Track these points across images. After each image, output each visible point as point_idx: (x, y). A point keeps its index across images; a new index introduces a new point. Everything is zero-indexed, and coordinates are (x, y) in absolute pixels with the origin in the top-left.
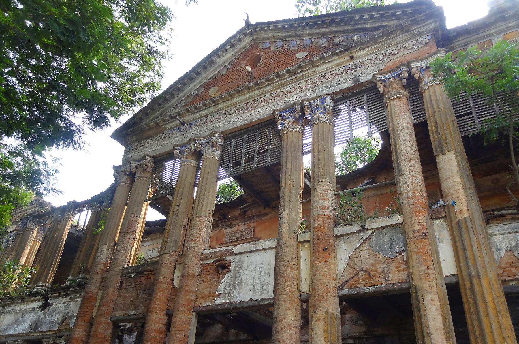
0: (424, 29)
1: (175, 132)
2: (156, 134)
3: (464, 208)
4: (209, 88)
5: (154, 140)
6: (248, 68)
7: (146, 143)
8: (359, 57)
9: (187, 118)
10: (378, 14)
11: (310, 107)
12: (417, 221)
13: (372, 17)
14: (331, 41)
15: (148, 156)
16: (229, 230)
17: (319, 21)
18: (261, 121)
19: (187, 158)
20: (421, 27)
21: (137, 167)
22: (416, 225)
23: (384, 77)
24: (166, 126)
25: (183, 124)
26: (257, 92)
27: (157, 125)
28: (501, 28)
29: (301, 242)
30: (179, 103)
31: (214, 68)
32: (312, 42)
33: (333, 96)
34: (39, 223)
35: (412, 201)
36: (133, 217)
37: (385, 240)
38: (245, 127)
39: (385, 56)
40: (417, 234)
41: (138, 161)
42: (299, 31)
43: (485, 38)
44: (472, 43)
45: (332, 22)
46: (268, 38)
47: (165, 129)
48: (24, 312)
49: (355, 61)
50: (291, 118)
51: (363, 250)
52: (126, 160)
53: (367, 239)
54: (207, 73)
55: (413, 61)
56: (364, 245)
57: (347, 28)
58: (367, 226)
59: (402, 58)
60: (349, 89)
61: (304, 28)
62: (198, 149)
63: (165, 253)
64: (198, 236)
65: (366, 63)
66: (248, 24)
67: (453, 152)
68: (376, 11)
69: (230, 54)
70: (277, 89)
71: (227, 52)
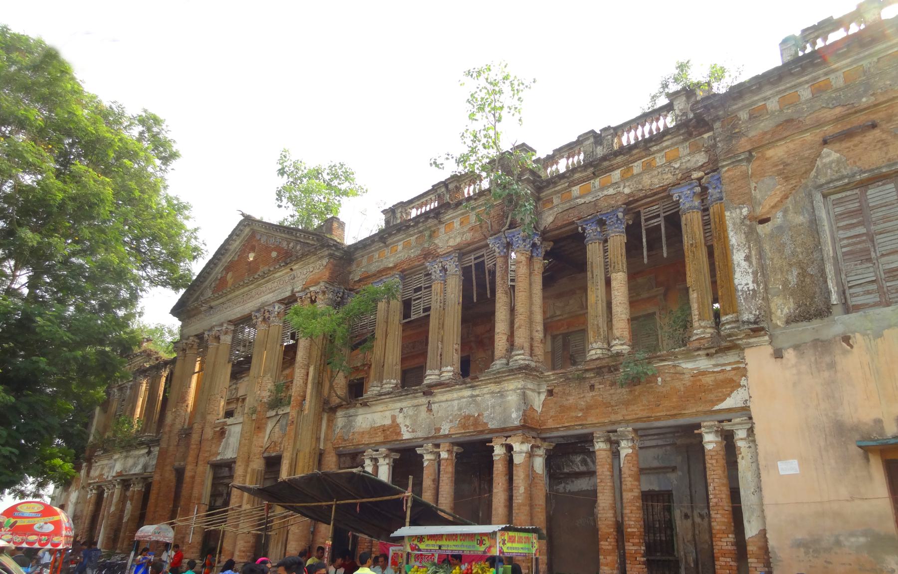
9: (213, 304)
25: (211, 308)
26: (246, 289)
33: (281, 302)
34: (145, 377)
48: (139, 457)
69: (238, 242)
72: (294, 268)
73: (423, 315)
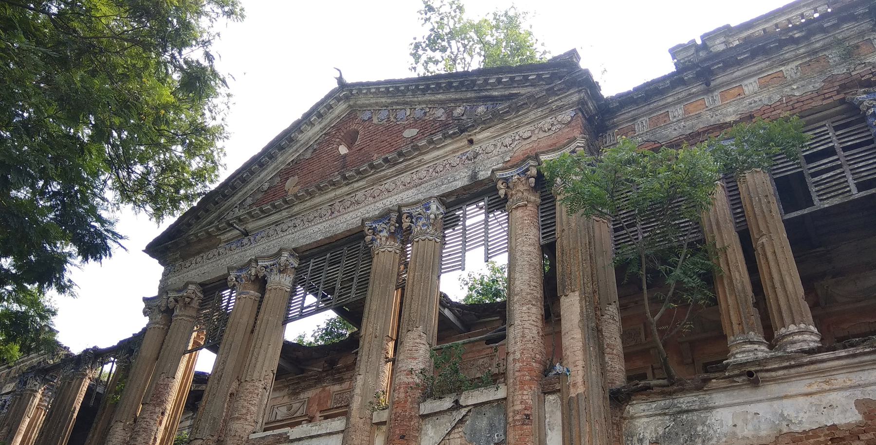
0: (565, 101)
1: (233, 247)
2: (209, 249)
3: (579, 379)
4: (287, 179)
5: (205, 257)
6: (343, 150)
7: (194, 262)
8: (480, 141)
9: (250, 226)
10: (506, 77)
11: (410, 216)
12: (520, 397)
13: (499, 81)
14: (450, 114)
15: (192, 283)
16: (337, 388)
17: (433, 84)
18: (348, 234)
19: (245, 288)
20: (560, 99)
21: (176, 301)
22: (519, 402)
23: (506, 174)
24: (222, 237)
25: (246, 234)
26: (346, 189)
27: (209, 235)
28: (680, 96)
29: (377, 424)
30: (244, 200)
31: (295, 148)
32: (425, 113)
33: (442, 199)
34: (45, 381)
35: (518, 365)
36: (163, 380)
37: (483, 423)
38: (327, 242)
39: (514, 140)
40: (518, 417)
41: (179, 291)
42: (409, 98)
43: (660, 110)
44: (643, 116)
45: (450, 86)
46: (370, 105)
47: (220, 241)
49: (476, 148)
50: (385, 231)
51: (454, 438)
52: (164, 288)
53: (461, 421)
54: (285, 156)
55: (543, 153)
56: (456, 430)
57: (470, 95)
58: (462, 402)
59: (535, 145)
60: (464, 188)
61: (414, 92)
62: (261, 275)
63: (196, 439)
64: (244, 411)
65: (489, 150)
66: (342, 84)
67: (577, 293)
68: (505, 73)
69: (317, 128)
70: (373, 185)
71: (312, 124)
72: (474, 138)
73: (856, 194)
